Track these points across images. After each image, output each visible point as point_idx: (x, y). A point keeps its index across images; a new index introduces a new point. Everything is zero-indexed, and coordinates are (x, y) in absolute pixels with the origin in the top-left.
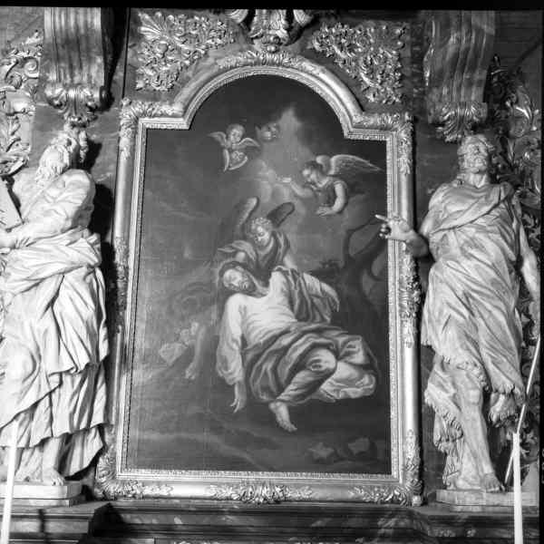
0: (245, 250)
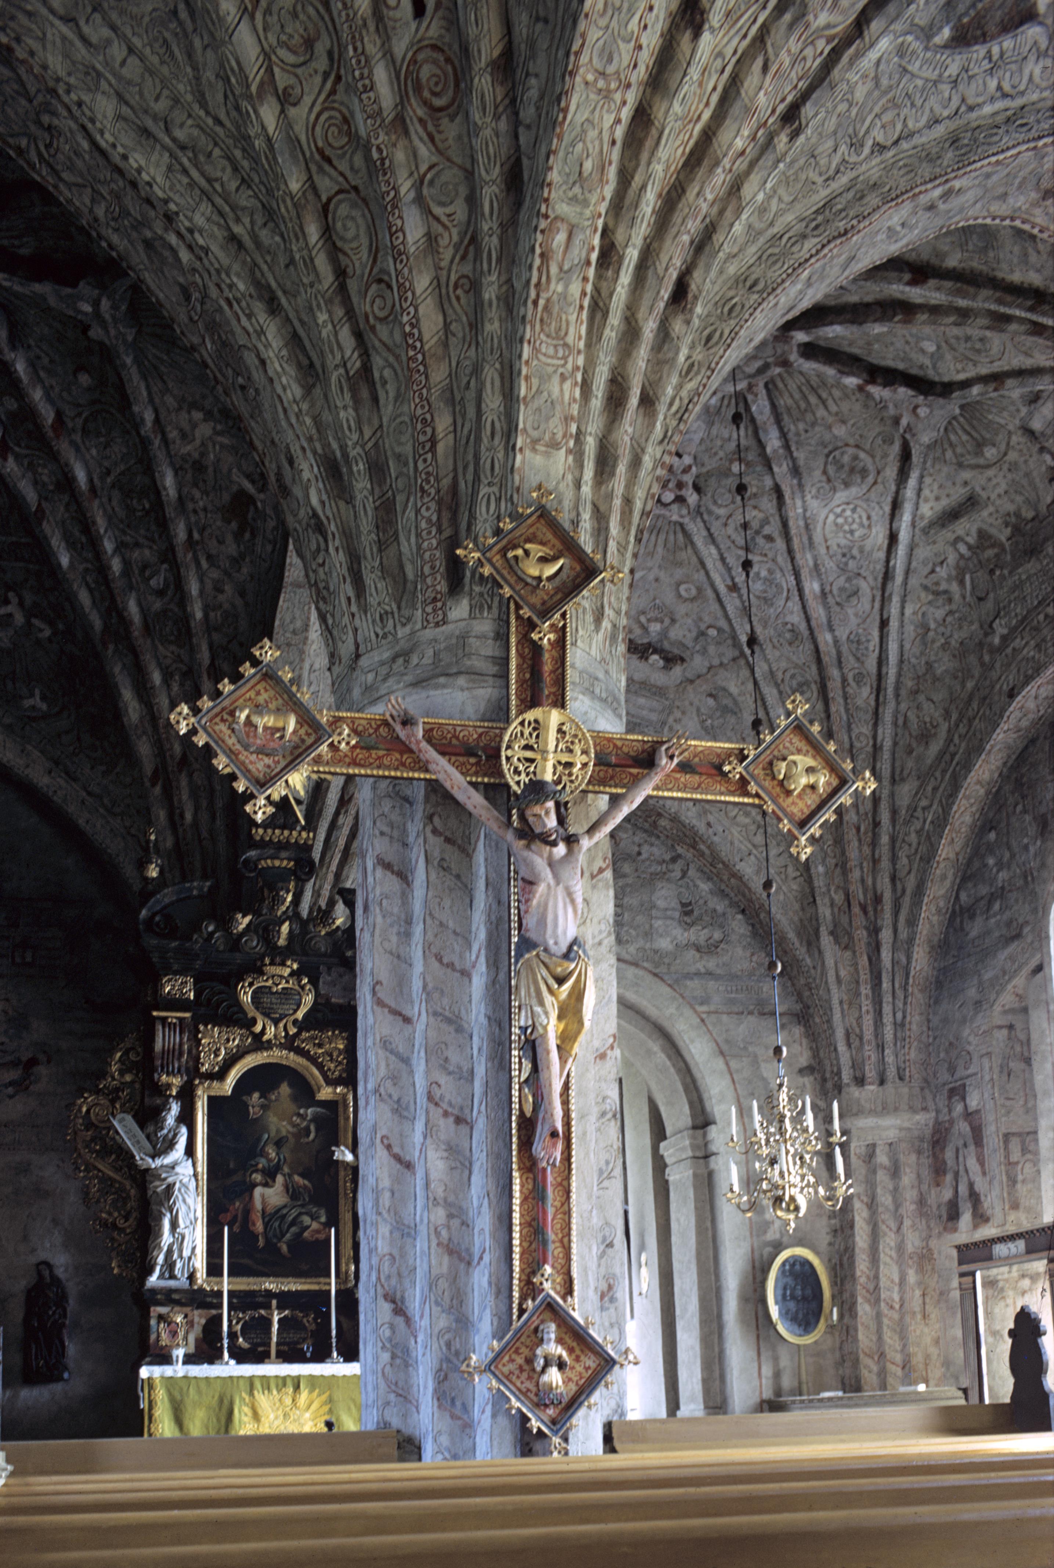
0: (262, 1163)
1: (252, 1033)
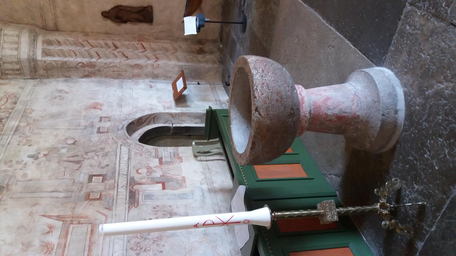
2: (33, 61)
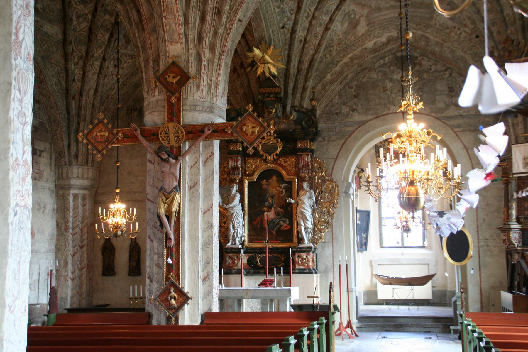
1: (263, 159)
2: (70, 187)
